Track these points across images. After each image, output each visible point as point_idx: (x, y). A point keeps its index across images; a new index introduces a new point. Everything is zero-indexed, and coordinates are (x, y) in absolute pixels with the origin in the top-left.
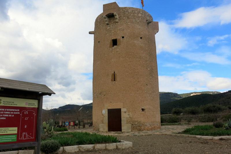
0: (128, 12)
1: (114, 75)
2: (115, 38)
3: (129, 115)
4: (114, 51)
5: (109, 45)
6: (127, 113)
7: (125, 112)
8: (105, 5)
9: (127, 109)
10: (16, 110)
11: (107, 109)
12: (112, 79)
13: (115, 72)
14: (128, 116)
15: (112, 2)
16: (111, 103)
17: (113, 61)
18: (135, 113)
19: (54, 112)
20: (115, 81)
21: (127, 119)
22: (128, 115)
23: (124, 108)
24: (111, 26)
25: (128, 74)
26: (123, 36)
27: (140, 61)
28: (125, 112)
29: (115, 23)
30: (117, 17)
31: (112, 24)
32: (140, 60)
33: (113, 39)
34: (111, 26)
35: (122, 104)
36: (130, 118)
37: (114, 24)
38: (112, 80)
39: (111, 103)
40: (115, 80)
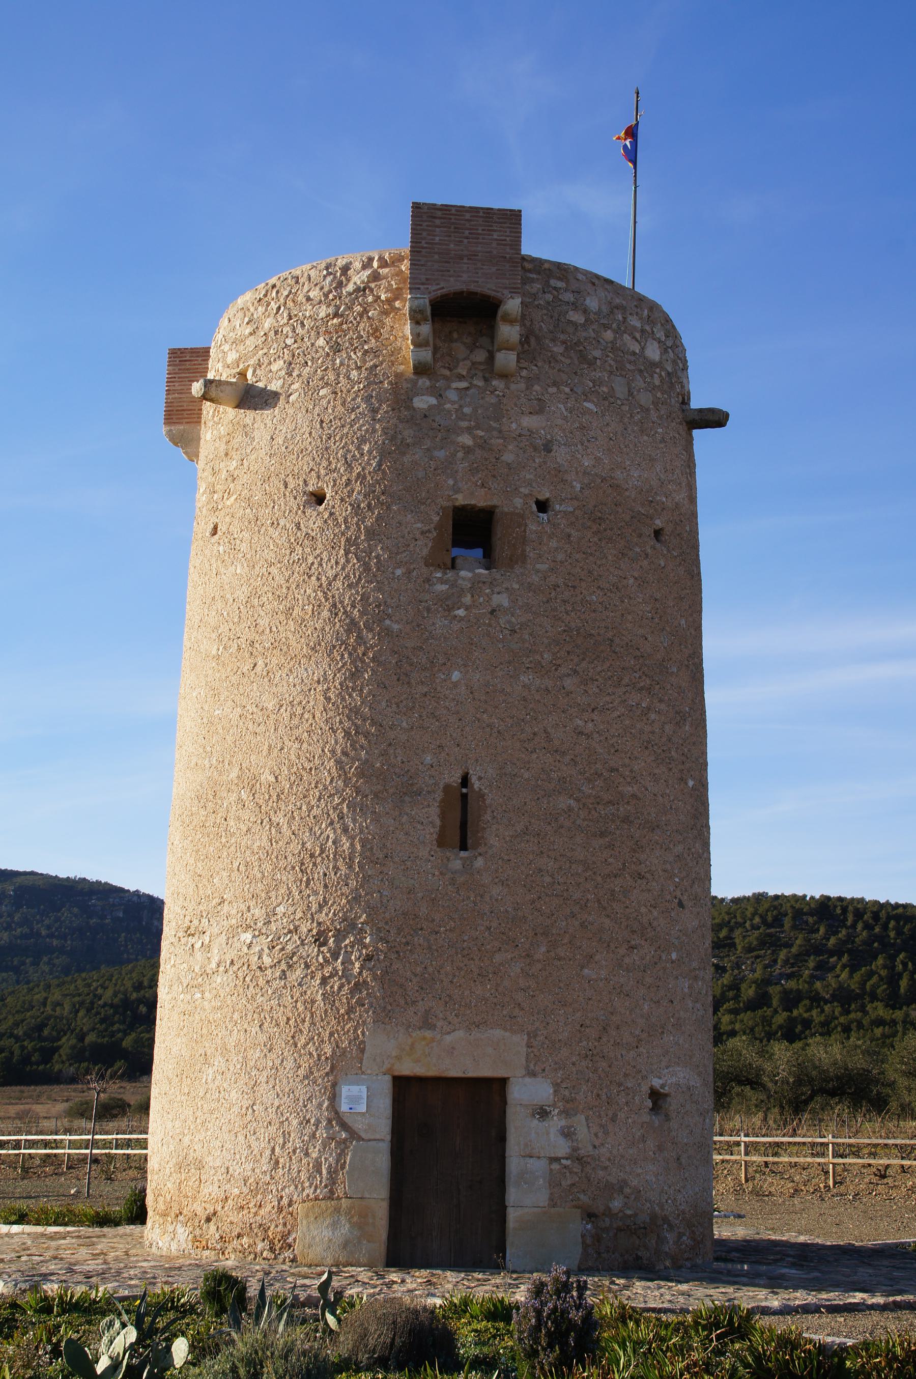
0: (585, 311)
1: (464, 797)
2: (480, 500)
3: (567, 1133)
4: (467, 599)
5: (423, 548)
6: (556, 1122)
7: (543, 1113)
8: (433, 207)
9: (557, 1086)
10: (858, 1297)
11: (388, 1078)
12: (443, 828)
13: (474, 779)
14: (562, 1148)
15: (468, 204)
16: (432, 1027)
17: (456, 685)
18: (614, 1119)
19: (722, 1242)
20: (464, 847)
21: (555, 1166)
22: (561, 1141)
23: (533, 1074)
24: (452, 395)
25: (570, 809)
26: (545, 495)
27: (653, 716)
28: (543, 1113)
29: (486, 380)
30: (508, 332)
31: (461, 378)
32: (649, 709)
33: (461, 500)
34: (452, 395)
35: (519, 1041)
36: (579, 1159)
37: (480, 383)
38: (442, 842)
39: (426, 1024)
40: (469, 842)
